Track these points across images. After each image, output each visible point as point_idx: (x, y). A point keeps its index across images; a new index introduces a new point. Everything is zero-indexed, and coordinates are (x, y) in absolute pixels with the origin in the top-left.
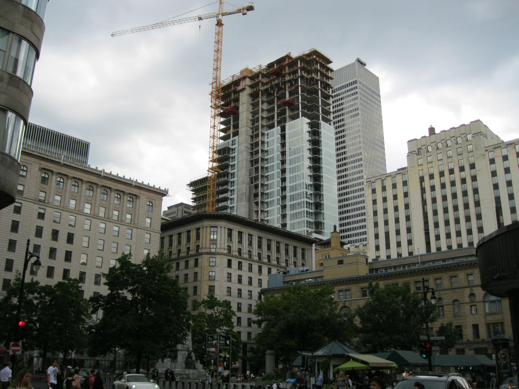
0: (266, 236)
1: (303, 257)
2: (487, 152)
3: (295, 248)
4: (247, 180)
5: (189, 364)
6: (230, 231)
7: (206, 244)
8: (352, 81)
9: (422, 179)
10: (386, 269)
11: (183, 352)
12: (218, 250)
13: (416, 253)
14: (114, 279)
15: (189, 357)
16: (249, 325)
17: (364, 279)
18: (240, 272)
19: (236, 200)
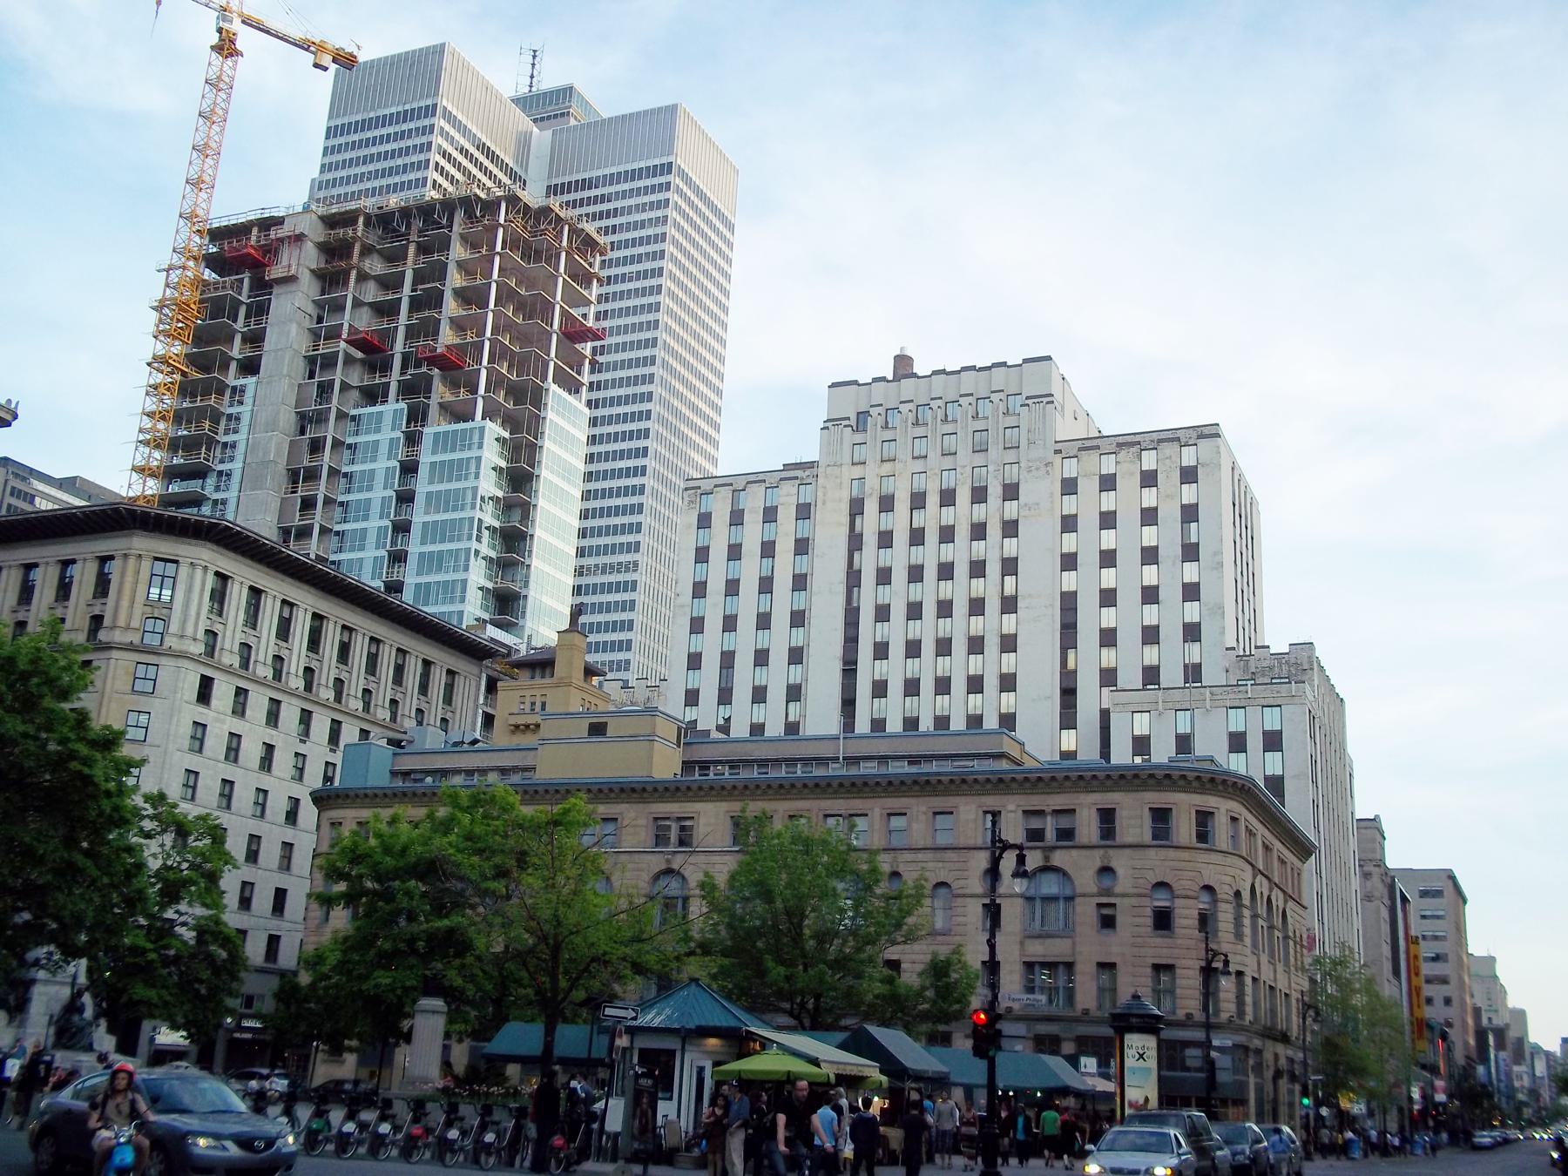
0: (338, 613)
1: (448, 700)
2: (1059, 456)
3: (427, 664)
4: (288, 419)
7: (130, 616)
8: (657, 162)
9: (856, 508)
10: (734, 765)
12: (170, 642)
13: (809, 729)
15: (73, 1007)
17: (655, 790)
18: (237, 725)
19: (236, 478)
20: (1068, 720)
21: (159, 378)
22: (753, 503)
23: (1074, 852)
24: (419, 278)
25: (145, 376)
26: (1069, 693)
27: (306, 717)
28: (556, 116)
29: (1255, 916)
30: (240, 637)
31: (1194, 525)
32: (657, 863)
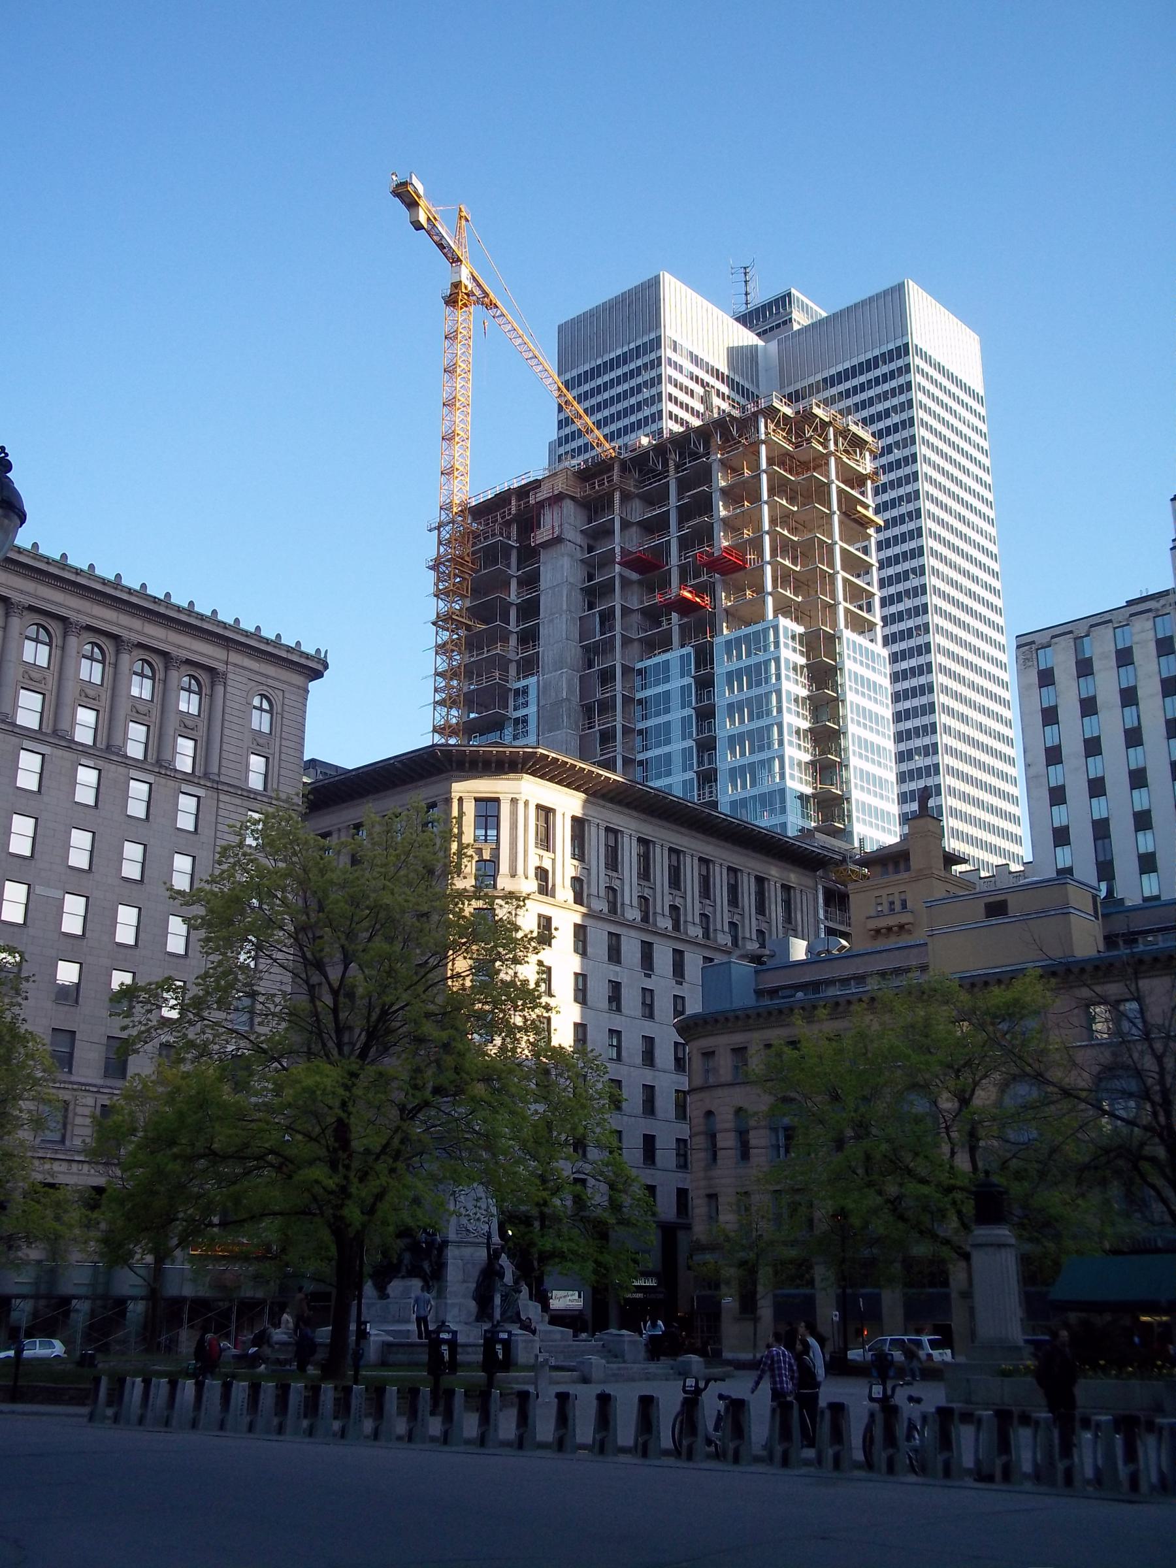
3: (760, 880)
4: (573, 652)
21: (445, 635)
22: (1102, 648)
24: (683, 486)
25: (430, 637)
27: (647, 951)
28: (778, 326)
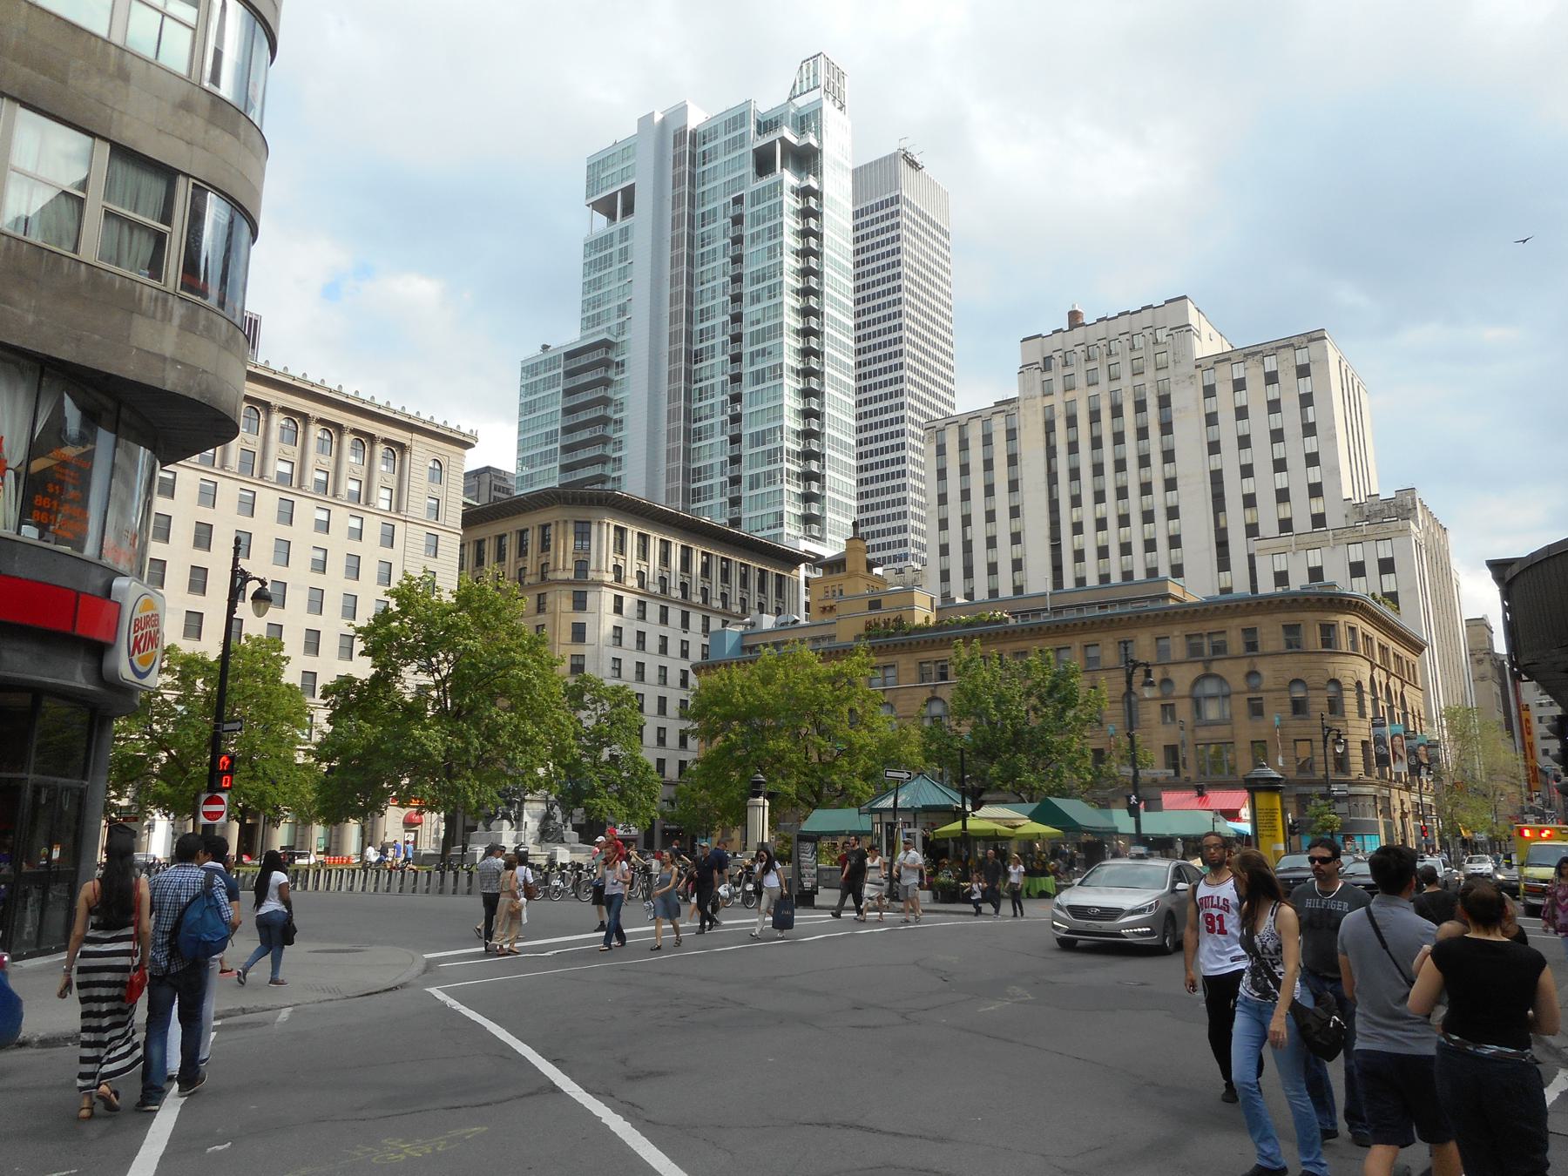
1: (780, 593)
5: (547, 833)
6: (620, 531)
8: (888, 196)
9: (1050, 427)
11: (535, 805)
14: (382, 640)
15: (547, 818)
16: (683, 742)
20: (1224, 564)
22: (975, 433)
23: (1227, 663)
26: (1222, 545)
29: (1375, 701)
30: (636, 568)
31: (1310, 409)
32: (925, 694)
